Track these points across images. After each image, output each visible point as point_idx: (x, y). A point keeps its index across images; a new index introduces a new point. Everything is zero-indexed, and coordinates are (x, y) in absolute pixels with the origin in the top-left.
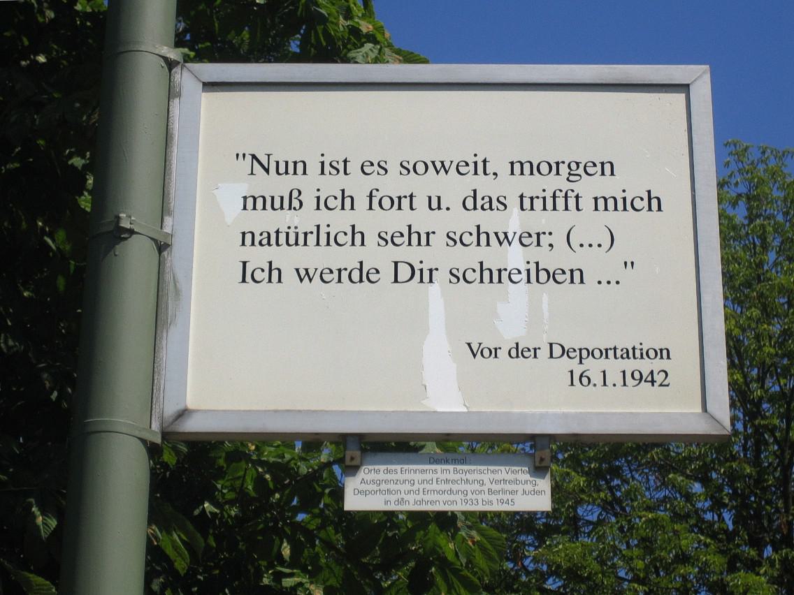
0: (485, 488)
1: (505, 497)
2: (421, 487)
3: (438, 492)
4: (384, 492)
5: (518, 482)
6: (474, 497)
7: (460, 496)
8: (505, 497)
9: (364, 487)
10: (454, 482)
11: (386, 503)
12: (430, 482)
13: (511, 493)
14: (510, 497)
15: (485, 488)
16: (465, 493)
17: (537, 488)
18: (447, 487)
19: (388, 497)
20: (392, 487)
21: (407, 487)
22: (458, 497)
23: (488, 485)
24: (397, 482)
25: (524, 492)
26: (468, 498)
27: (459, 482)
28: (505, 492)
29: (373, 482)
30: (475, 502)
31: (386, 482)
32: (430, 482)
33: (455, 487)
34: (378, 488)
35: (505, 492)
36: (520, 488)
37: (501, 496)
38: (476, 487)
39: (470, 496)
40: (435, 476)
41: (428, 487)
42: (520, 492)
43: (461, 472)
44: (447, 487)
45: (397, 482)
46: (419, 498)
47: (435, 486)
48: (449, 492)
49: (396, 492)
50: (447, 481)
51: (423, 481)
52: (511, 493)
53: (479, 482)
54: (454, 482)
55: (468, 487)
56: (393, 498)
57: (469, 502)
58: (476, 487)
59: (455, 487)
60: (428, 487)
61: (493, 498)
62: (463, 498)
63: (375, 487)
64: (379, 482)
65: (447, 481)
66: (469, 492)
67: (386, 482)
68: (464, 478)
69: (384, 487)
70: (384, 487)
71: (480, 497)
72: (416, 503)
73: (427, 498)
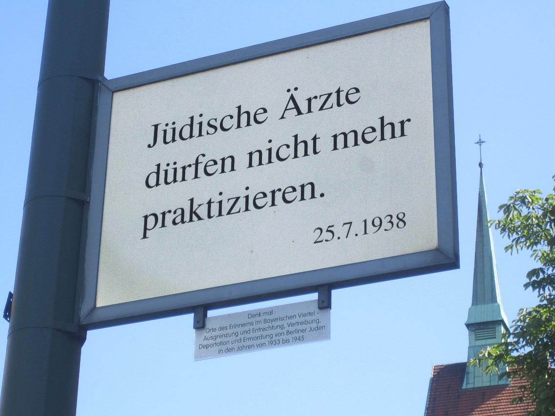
0: (285, 331)
1: (297, 335)
2: (242, 337)
4: (218, 345)
6: (278, 338)
8: (297, 335)
10: (264, 329)
13: (303, 331)
14: (301, 334)
15: (285, 331)
16: (271, 336)
17: (319, 325)
18: (258, 334)
20: (225, 339)
21: (234, 338)
23: (287, 328)
24: (226, 336)
26: (273, 340)
27: (267, 329)
33: (265, 333)
36: (307, 327)
38: (279, 330)
40: (251, 327)
41: (248, 336)
43: (269, 321)
45: (226, 336)
47: (252, 335)
52: (303, 331)
53: (280, 327)
54: (264, 329)
55: (273, 332)
58: (279, 330)
59: (265, 333)
60: (248, 336)
62: (270, 340)
66: (274, 336)
68: (271, 325)
70: (219, 340)
71: (280, 338)
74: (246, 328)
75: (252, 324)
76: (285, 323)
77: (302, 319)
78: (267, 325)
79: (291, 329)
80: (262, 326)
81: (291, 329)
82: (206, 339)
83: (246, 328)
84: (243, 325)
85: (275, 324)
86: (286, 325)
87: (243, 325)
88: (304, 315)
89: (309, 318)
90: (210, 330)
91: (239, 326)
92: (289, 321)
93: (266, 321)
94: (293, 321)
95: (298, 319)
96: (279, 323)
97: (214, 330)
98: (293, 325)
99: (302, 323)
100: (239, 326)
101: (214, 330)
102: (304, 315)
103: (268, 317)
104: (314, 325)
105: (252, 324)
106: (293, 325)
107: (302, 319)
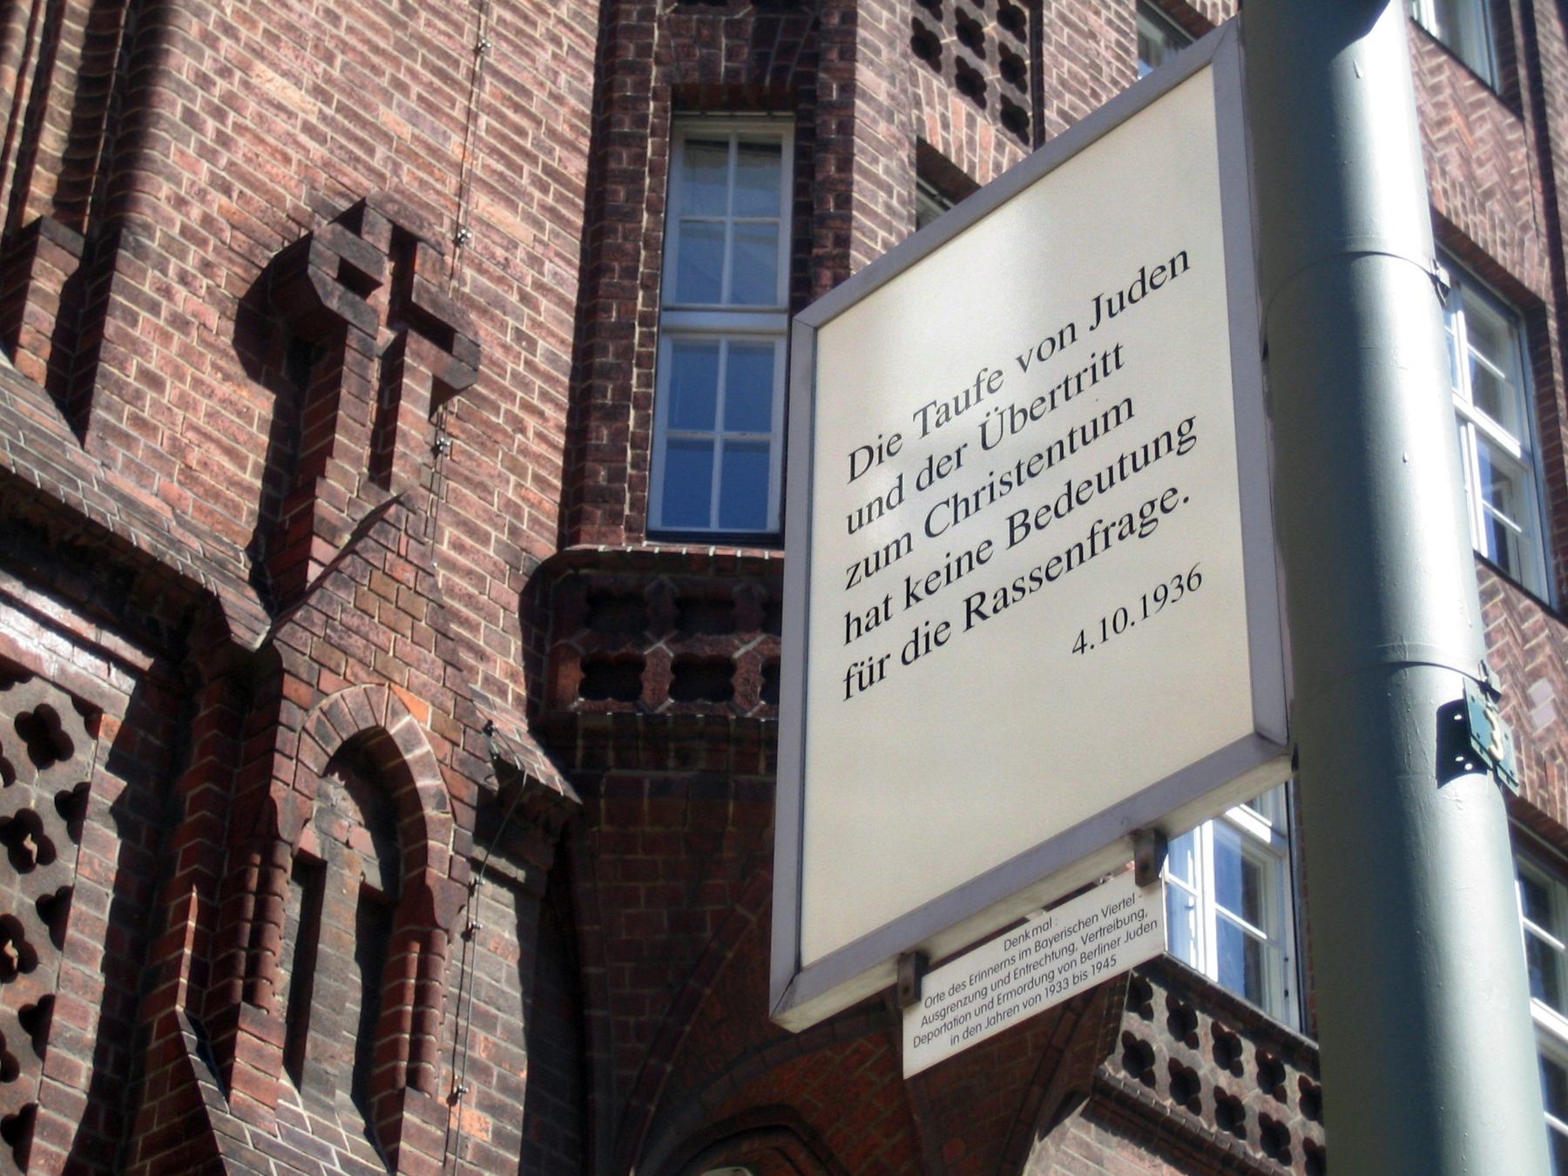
0: (1077, 956)
1: (1102, 958)
3: (1017, 992)
7: (1046, 984)
8: (1102, 958)
13: (1111, 946)
14: (1108, 954)
15: (1077, 956)
16: (1050, 976)
17: (1146, 921)
20: (961, 1011)
21: (979, 1002)
22: (1040, 989)
25: (1129, 937)
28: (1101, 949)
29: (938, 1015)
33: (1036, 974)
35: (1101, 949)
38: (1066, 958)
39: (1058, 978)
40: (1011, 969)
41: (1004, 989)
47: (1014, 984)
51: (997, 985)
58: (1066, 958)
59: (1036, 974)
61: (1087, 966)
63: (938, 1023)
67: (952, 1007)
69: (950, 1017)
70: (950, 1017)
74: (1002, 974)
76: (1075, 938)
77: (1110, 919)
79: (1091, 946)
81: (1091, 946)
82: (926, 1021)
83: (1002, 974)
84: (994, 970)
90: (933, 1001)
91: (987, 973)
92: (1084, 932)
93: (1038, 946)
95: (1104, 922)
96: (1065, 942)
97: (940, 997)
98: (1092, 937)
100: (987, 973)
106: (1092, 937)
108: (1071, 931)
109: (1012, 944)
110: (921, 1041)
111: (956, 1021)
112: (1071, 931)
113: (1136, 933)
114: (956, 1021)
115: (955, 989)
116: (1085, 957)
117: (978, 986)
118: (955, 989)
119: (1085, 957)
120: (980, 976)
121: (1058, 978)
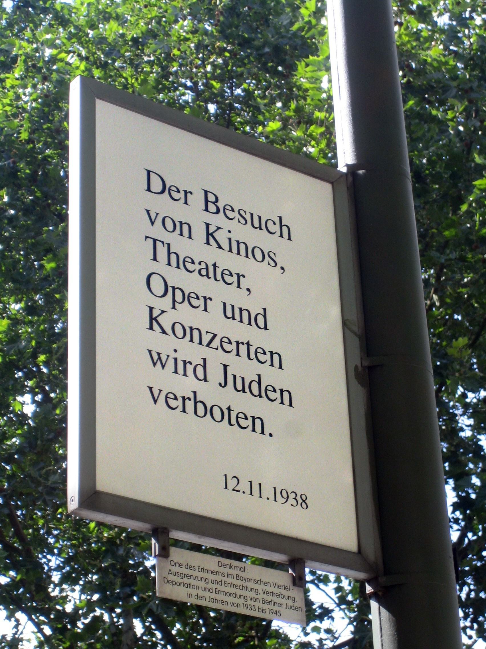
1: (275, 608)
2: (215, 586)
5: (282, 596)
6: (252, 603)
9: (171, 577)
10: (237, 587)
11: (189, 595)
12: (220, 583)
17: (296, 605)
18: (233, 590)
19: (191, 591)
22: (241, 601)
24: (196, 578)
25: (287, 607)
28: (274, 604)
29: (177, 574)
30: (253, 608)
31: (189, 576)
32: (220, 583)
33: (239, 592)
34: (181, 581)
35: (274, 604)
37: (271, 607)
42: (284, 606)
44: (233, 590)
45: (196, 578)
46: (213, 595)
48: (234, 596)
49: (196, 587)
50: (232, 585)
54: (237, 587)
56: (194, 592)
57: (249, 607)
59: (239, 592)
60: (220, 588)
62: (245, 603)
63: (178, 579)
64: (183, 576)
65: (232, 585)
66: (249, 599)
67: (189, 576)
68: (244, 585)
69: (186, 580)
70: (186, 580)
71: (257, 604)
72: (210, 600)
73: (220, 597)
74: (218, 578)
75: (223, 575)
76: (260, 587)
77: (277, 591)
78: (239, 583)
80: (235, 581)
82: (170, 572)
83: (218, 578)
84: (213, 572)
85: (250, 585)
86: (260, 591)
87: (213, 572)
88: (279, 586)
89: (284, 592)
92: (264, 587)
93: (238, 577)
94: (269, 589)
96: (256, 586)
97: (180, 565)
99: (277, 595)
101: (180, 565)
102: (279, 586)
103: (241, 574)
104: (290, 603)
105: (223, 575)
107: (277, 591)
108: (256, 582)
109: (223, 565)
110: (169, 582)
111: (190, 586)
112: (256, 582)
113: (291, 607)
114: (190, 586)
115: (189, 567)
116: (264, 601)
117: (205, 575)
118: (189, 567)
119: (264, 601)
120: (205, 570)
121: (249, 602)
